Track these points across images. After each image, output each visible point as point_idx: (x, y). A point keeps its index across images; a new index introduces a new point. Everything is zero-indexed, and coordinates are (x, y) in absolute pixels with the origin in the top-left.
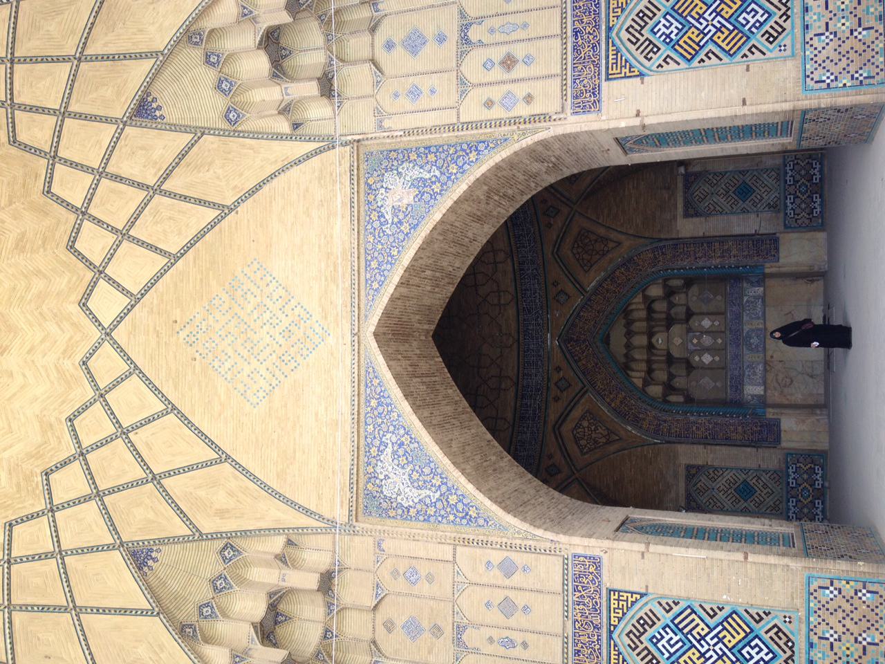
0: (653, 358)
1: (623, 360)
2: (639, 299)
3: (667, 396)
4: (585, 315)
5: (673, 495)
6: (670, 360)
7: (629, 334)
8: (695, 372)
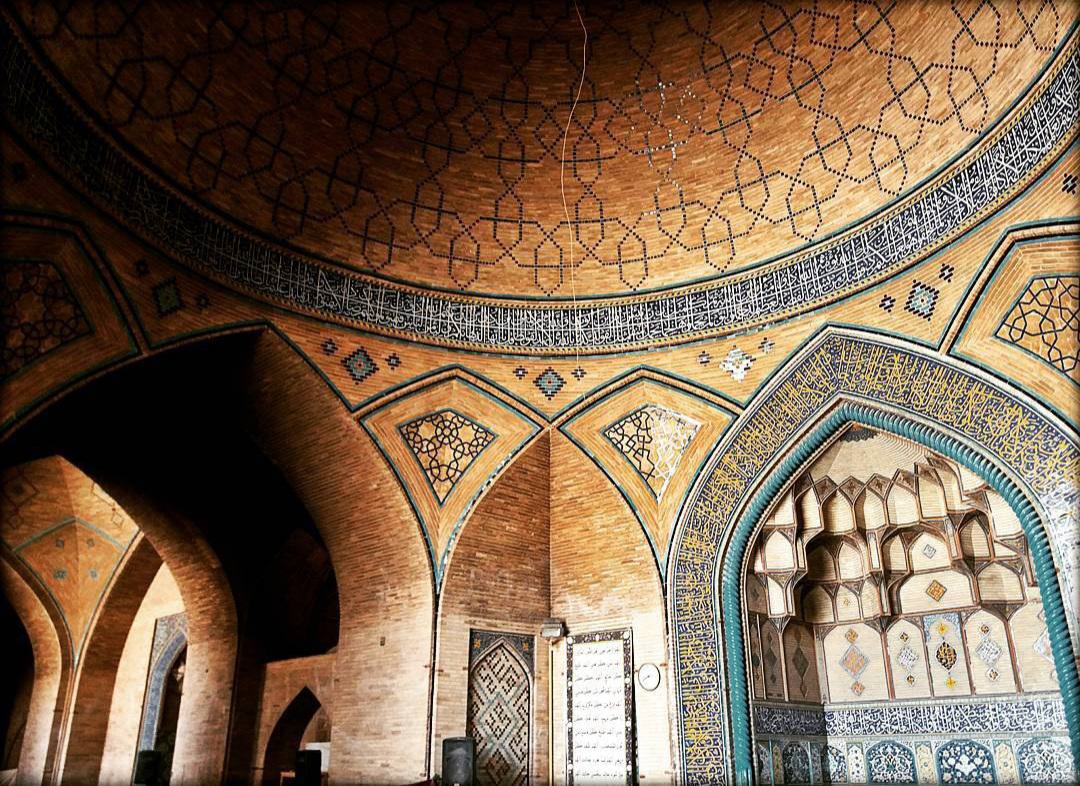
0: (873, 543)
1: (838, 479)
2: (972, 482)
3: (773, 578)
4: (896, 368)
5: (586, 610)
6: (888, 579)
7: (911, 480)
8: (875, 635)
